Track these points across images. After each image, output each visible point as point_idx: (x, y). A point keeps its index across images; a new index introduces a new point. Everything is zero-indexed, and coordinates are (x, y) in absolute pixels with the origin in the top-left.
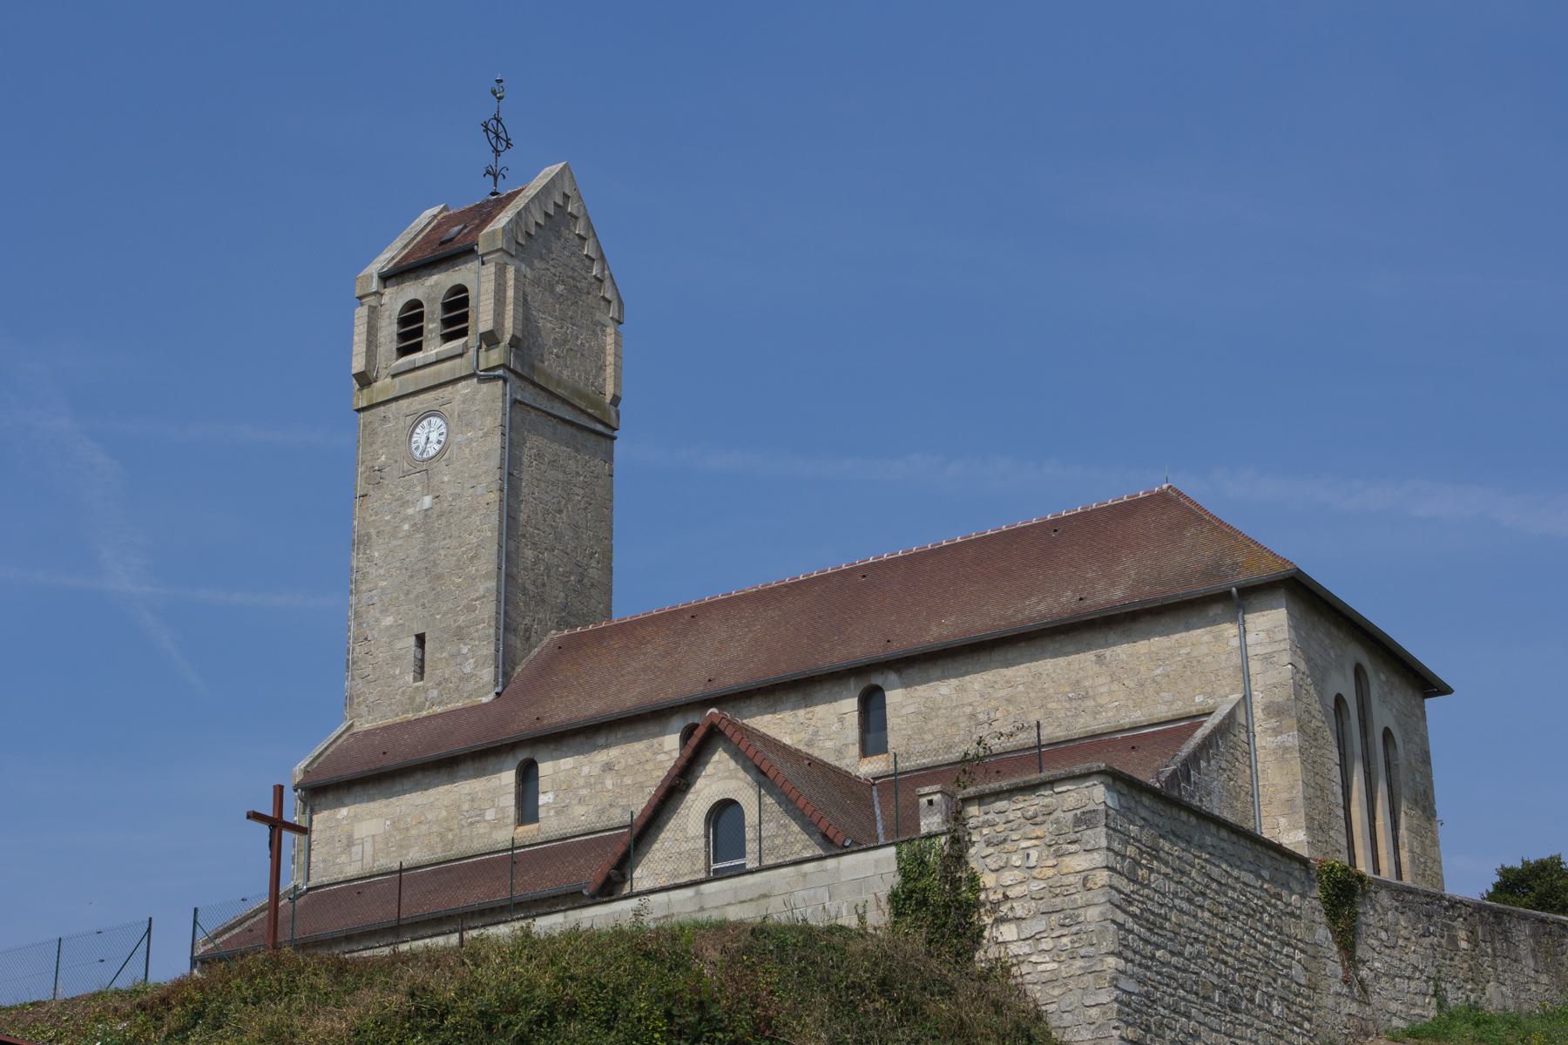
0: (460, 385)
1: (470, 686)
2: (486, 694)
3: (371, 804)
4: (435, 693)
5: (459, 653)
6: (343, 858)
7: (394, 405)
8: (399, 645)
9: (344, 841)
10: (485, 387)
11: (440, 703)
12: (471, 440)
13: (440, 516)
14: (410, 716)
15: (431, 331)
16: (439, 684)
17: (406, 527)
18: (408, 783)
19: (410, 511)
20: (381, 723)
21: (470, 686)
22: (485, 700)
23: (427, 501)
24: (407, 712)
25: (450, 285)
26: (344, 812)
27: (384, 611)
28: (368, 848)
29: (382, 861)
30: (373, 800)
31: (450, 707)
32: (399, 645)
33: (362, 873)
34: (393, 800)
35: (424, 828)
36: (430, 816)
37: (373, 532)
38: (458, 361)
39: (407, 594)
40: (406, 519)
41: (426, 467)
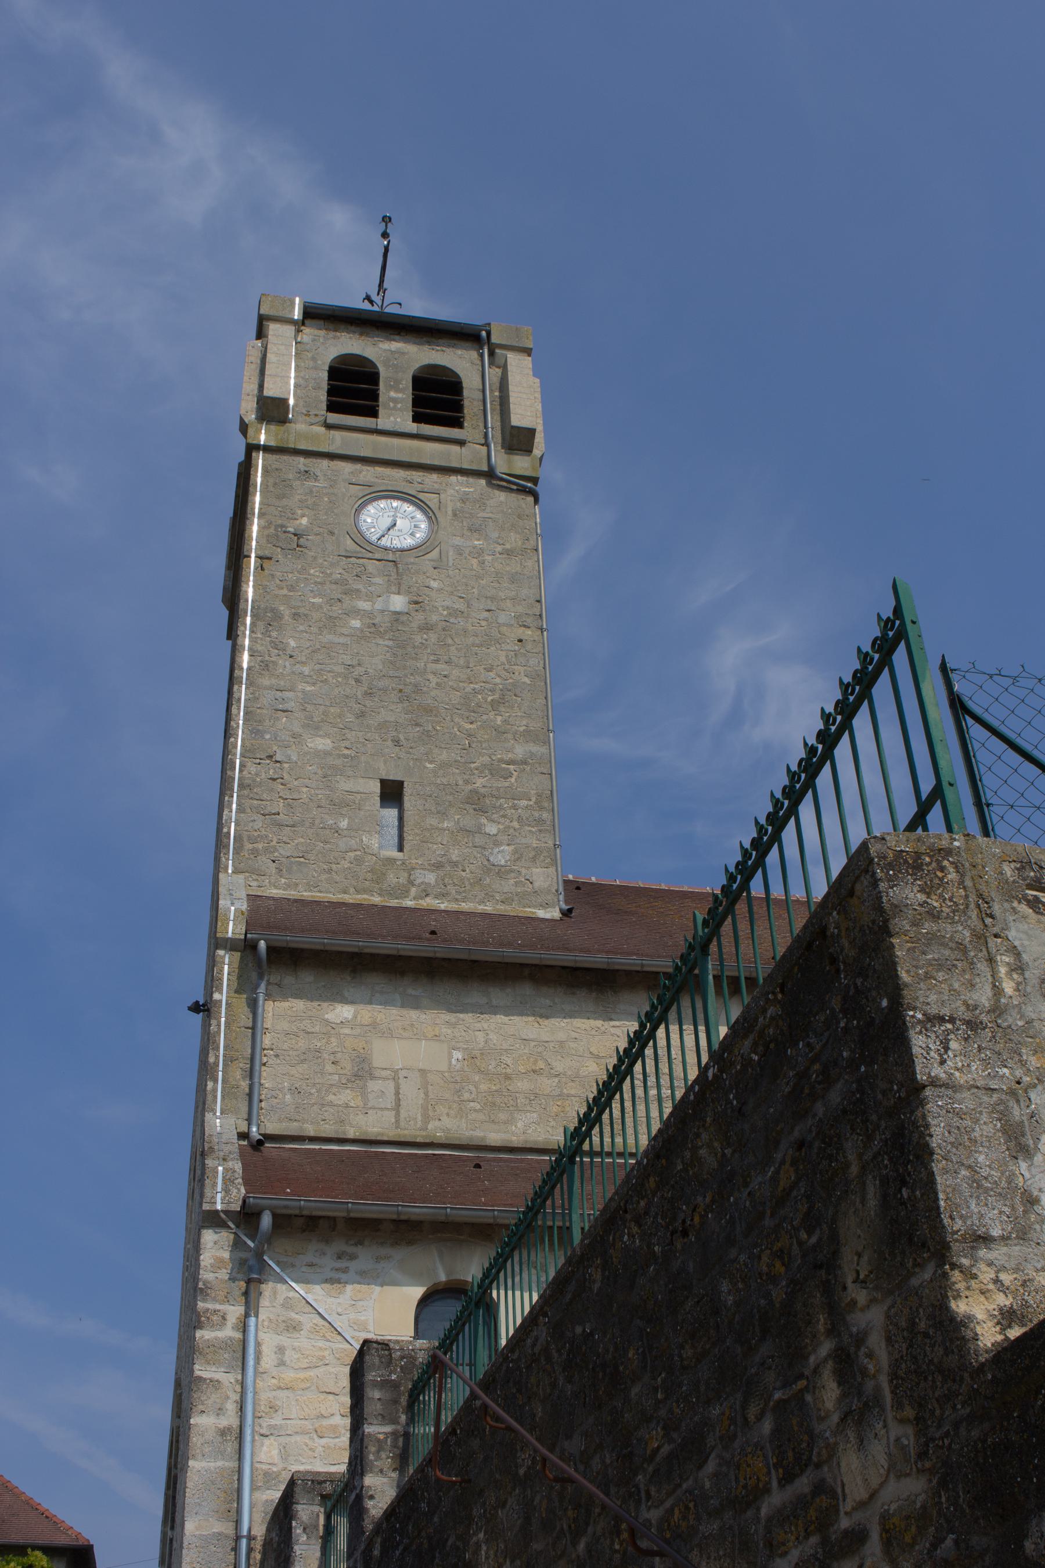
0: (453, 479)
1: (508, 885)
2: (545, 906)
3: (413, 1014)
4: (431, 878)
5: (479, 830)
6: (346, 1096)
7: (325, 463)
8: (345, 785)
9: (348, 1067)
10: (502, 496)
11: (442, 896)
12: (479, 553)
13: (427, 627)
14: (376, 900)
15: (395, 401)
16: (438, 866)
17: (356, 623)
18: (498, 995)
19: (364, 605)
20: (292, 894)
21: (508, 885)
22: (541, 914)
23: (398, 602)
24: (365, 891)
25: (426, 361)
26: (344, 1012)
27: (314, 727)
28: (411, 1091)
29: (447, 1122)
30: (417, 1007)
31: (465, 906)
32: (345, 785)
33: (391, 1134)
34: (468, 1017)
35: (547, 1084)
36: (559, 1066)
37: (286, 612)
38: (455, 449)
39: (362, 715)
40: (356, 612)
41: (396, 562)
